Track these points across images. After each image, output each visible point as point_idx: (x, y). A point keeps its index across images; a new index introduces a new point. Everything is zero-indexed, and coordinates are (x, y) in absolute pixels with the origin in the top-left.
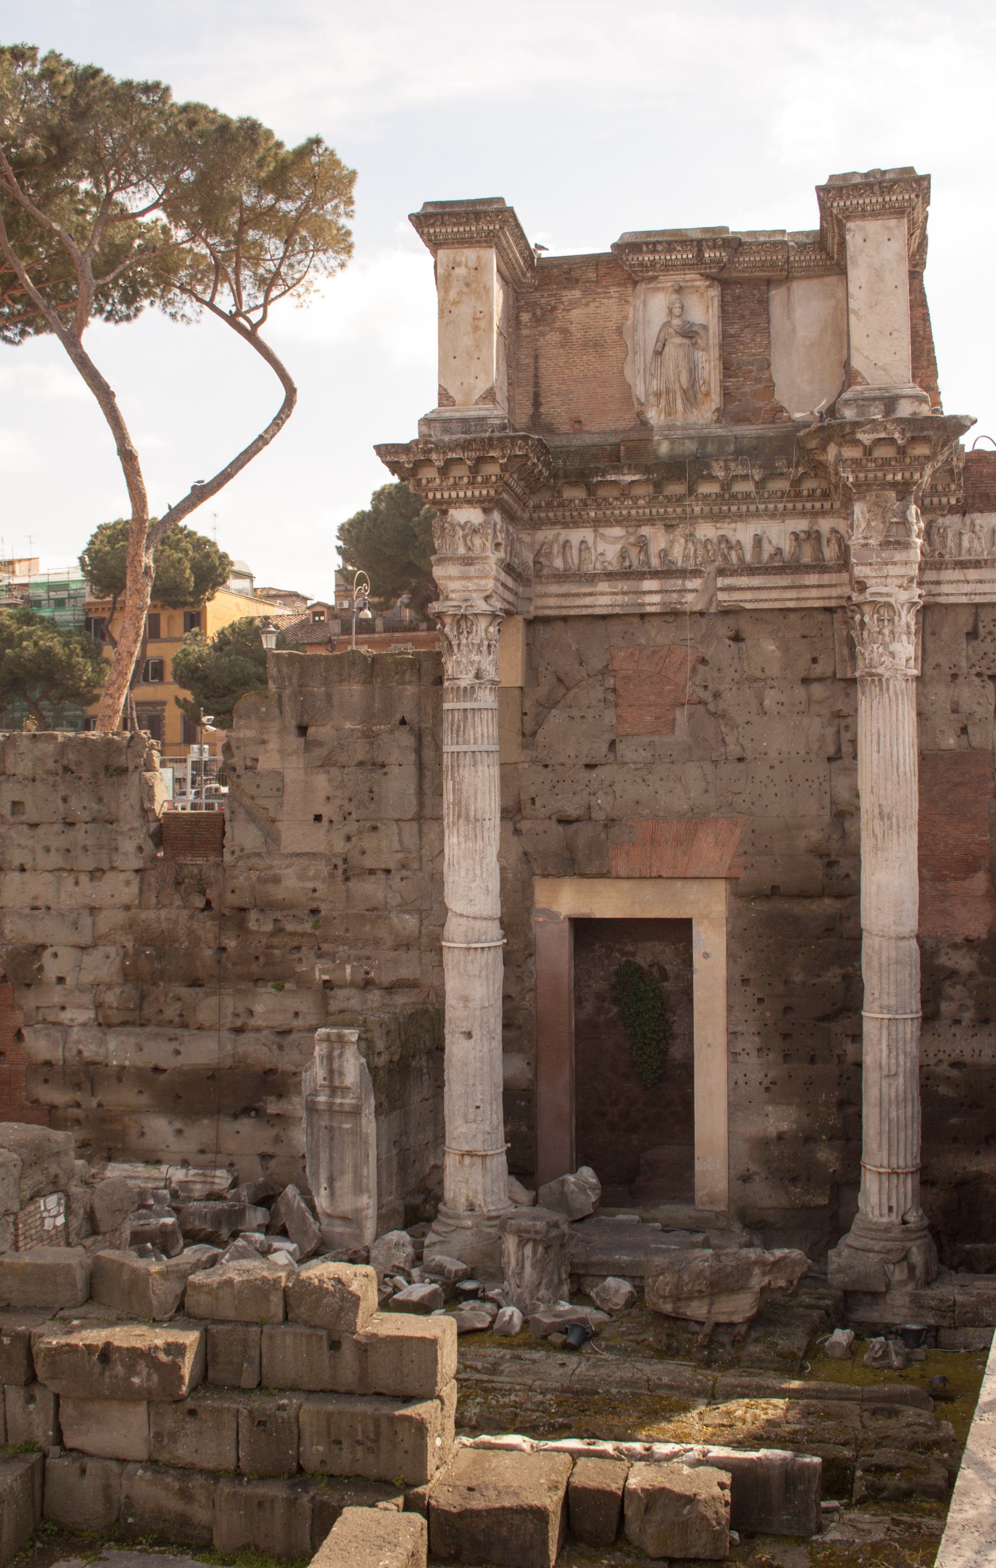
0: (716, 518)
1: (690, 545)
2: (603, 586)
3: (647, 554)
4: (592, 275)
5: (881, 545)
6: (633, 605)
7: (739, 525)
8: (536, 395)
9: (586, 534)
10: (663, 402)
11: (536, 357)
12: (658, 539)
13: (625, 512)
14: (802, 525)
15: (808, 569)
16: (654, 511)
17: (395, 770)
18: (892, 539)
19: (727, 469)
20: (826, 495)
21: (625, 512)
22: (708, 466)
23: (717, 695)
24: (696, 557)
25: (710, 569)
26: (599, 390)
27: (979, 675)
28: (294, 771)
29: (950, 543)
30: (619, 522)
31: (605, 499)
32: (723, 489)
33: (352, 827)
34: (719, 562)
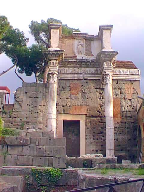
0: (84, 67)
4: (69, 37)
7: (87, 68)
9: (67, 68)
12: (76, 69)
14: (95, 69)
15: (97, 74)
17: (39, 98)
20: (99, 65)
23: (84, 90)
27: (118, 89)
28: (25, 98)
29: (114, 71)
30: (72, 67)
33: (33, 106)
34: (85, 73)
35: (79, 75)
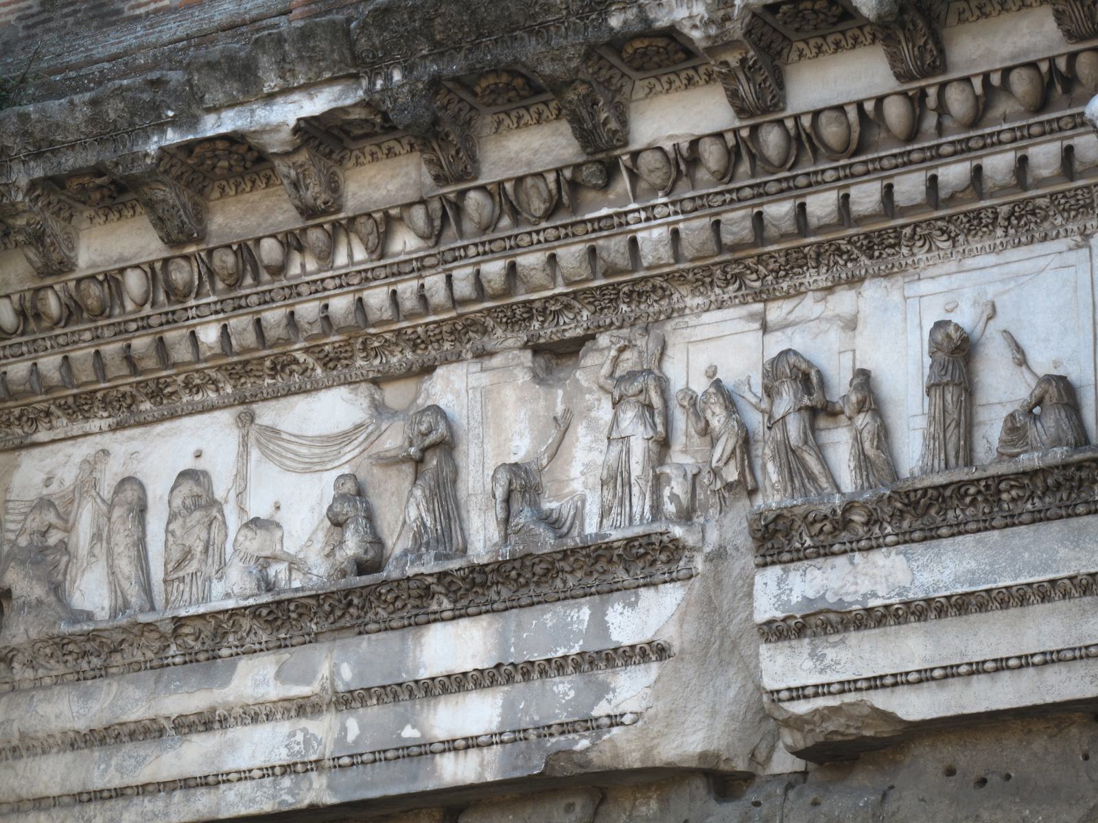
1: (629, 416)
2: (255, 678)
3: (445, 496)
6: (379, 757)
7: (873, 298)
9: (203, 439)
13: (340, 304)
16: (463, 276)
21: (340, 304)
24: (658, 482)
25: (728, 528)
31: (245, 252)
32: (741, 110)
35: (564, 625)
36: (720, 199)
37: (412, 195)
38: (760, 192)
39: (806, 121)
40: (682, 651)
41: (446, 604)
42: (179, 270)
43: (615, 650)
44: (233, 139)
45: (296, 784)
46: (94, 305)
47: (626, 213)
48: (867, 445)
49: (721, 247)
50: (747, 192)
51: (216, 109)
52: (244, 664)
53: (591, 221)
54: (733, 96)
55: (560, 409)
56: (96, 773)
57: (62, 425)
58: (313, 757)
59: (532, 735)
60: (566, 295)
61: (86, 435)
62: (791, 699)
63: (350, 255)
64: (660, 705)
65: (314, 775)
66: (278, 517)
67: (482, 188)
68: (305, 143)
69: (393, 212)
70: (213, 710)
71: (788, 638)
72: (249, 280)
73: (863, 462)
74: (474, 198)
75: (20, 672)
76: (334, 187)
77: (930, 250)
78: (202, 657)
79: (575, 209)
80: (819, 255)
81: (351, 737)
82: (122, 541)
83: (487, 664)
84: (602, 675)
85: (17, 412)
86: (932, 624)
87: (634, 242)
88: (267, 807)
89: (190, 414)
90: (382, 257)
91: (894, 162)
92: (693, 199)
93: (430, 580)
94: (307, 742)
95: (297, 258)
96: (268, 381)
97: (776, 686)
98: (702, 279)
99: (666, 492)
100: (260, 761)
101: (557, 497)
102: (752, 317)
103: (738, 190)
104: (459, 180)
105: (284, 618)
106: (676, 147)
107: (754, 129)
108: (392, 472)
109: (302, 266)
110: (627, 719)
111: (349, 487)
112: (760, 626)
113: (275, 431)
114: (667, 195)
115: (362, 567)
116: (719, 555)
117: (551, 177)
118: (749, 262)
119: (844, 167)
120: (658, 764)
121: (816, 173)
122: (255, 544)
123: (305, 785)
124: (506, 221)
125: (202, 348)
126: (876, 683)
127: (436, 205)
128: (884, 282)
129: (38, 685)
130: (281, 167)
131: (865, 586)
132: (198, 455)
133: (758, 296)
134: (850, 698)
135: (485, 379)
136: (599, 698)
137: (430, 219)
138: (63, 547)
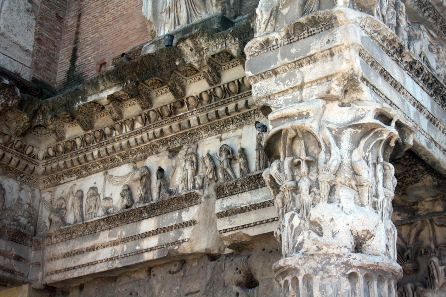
0: (217, 125)
2: (104, 237)
5: (288, 36)
6: (131, 254)
8: (75, 50)
9: (96, 179)
10: (172, 15)
11: (79, 16)
18: (303, 20)
19: (198, 50)
21: (124, 142)
22: (179, 54)
25: (210, 190)
26: (123, 27)
30: (125, 157)
32: (210, 84)
35: (171, 218)
36: (208, 108)
37: (138, 113)
38: (217, 105)
39: (226, 86)
40: (199, 222)
41: (146, 215)
42: (88, 137)
43: (183, 223)
44: (95, 102)
45: (113, 263)
46: (71, 147)
47: (187, 114)
48: (242, 166)
49: (209, 121)
50: (214, 106)
51: (90, 95)
52: (102, 233)
53: (179, 116)
54: (208, 80)
55: (174, 165)
56: (69, 263)
57: (66, 179)
58: (116, 256)
59: (165, 246)
60: (175, 136)
61: (71, 181)
62: (224, 232)
63: (126, 130)
64: (194, 236)
65: (116, 260)
66: (112, 197)
67: (153, 110)
68: (111, 102)
69: (134, 118)
70: (95, 245)
71: (223, 217)
72: (104, 139)
73: (241, 171)
74: (151, 113)
75: (54, 240)
76: (120, 113)
77: (258, 117)
78: (92, 232)
79: (176, 113)
80: (232, 121)
81: (125, 250)
82: (76, 205)
83: (155, 229)
84: (181, 230)
85: (55, 176)
86: (257, 211)
87: (189, 121)
88: (106, 269)
89: (94, 173)
90: (133, 130)
91: (247, 94)
92: (202, 109)
93: (142, 209)
94: (115, 252)
95: (114, 132)
96: (110, 164)
97: (220, 229)
98: (206, 130)
99: (196, 182)
100: (105, 258)
101: (172, 186)
102: (218, 138)
103: (212, 105)
104: (148, 108)
105: (112, 220)
106: (197, 95)
107: (214, 89)
108: (136, 183)
109: (116, 133)
110: (186, 240)
111: (126, 188)
112: (217, 214)
113: (112, 176)
114: (196, 108)
115: (127, 207)
116: (208, 197)
117: (169, 106)
118: (216, 123)
119: (236, 97)
120: (195, 252)
121: (229, 99)
122: (105, 204)
123: (114, 263)
124: (160, 118)
125: (94, 156)
126: (244, 227)
127: (143, 115)
128: (248, 126)
129: (57, 242)
130: (106, 108)
131: (241, 202)
132: (95, 183)
133: (219, 132)
134: (238, 231)
135: (158, 159)
136: (180, 236)
137: (142, 120)
138: (65, 208)
